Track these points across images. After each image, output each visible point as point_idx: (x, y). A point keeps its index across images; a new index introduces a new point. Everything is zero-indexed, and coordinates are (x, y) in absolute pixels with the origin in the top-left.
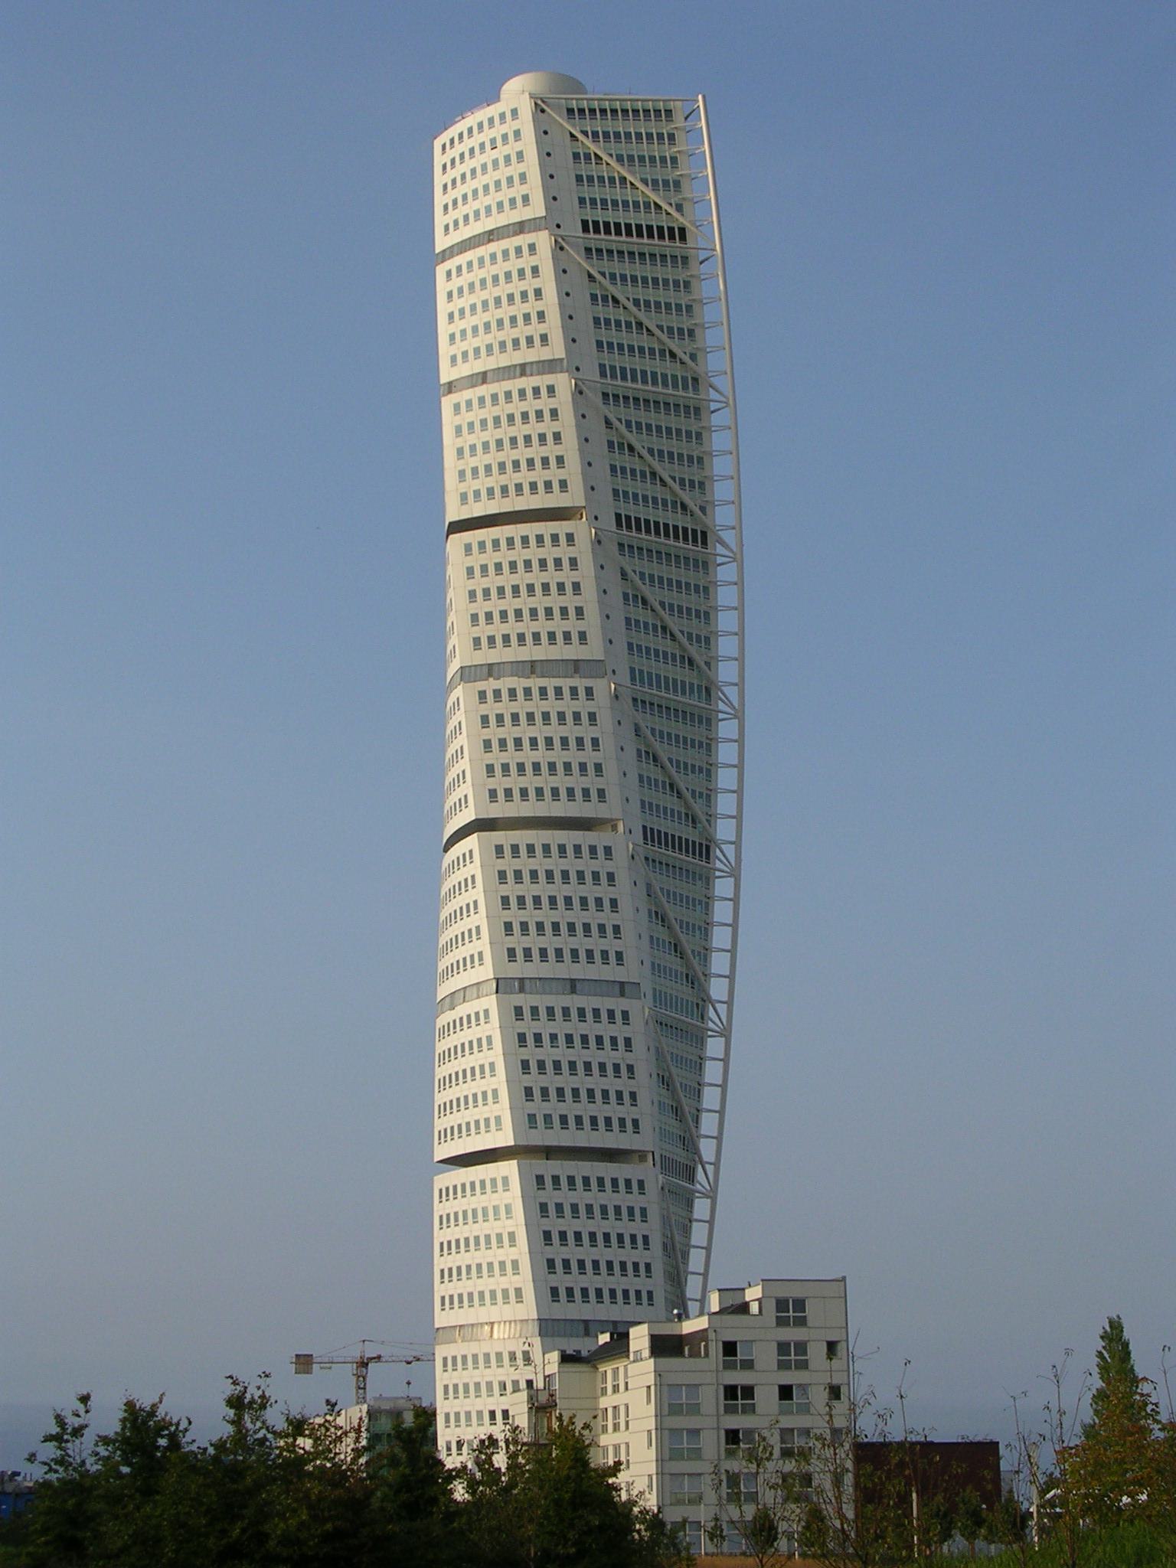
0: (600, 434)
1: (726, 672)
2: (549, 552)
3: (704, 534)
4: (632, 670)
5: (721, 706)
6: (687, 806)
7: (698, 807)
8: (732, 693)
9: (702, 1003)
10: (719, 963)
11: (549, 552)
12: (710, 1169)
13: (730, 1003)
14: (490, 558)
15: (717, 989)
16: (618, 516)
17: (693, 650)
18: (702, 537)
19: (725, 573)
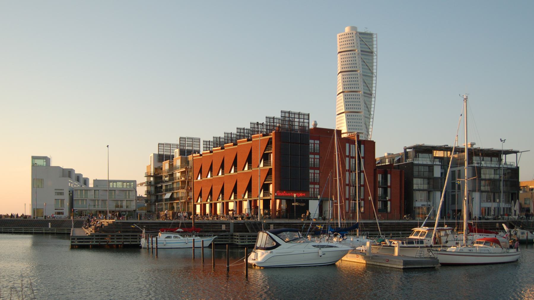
0: (359, 39)
1: (374, 71)
2: (352, 56)
3: (372, 52)
4: (362, 71)
5: (374, 76)
6: (368, 47)
7: (370, 89)
8: (375, 74)
9: (370, 114)
10: (372, 109)
11: (352, 56)
12: (370, 136)
13: (373, 115)
14: (344, 57)
15: (372, 113)
16: (361, 50)
17: (370, 68)
18: (372, 52)
19: (375, 57)
